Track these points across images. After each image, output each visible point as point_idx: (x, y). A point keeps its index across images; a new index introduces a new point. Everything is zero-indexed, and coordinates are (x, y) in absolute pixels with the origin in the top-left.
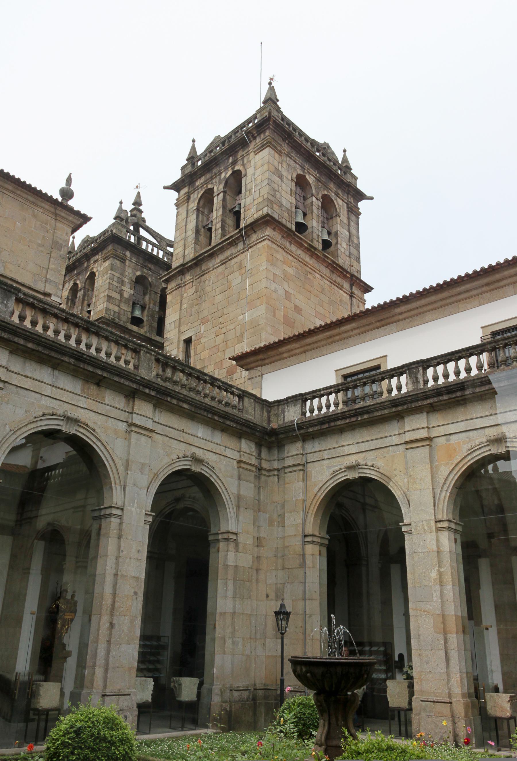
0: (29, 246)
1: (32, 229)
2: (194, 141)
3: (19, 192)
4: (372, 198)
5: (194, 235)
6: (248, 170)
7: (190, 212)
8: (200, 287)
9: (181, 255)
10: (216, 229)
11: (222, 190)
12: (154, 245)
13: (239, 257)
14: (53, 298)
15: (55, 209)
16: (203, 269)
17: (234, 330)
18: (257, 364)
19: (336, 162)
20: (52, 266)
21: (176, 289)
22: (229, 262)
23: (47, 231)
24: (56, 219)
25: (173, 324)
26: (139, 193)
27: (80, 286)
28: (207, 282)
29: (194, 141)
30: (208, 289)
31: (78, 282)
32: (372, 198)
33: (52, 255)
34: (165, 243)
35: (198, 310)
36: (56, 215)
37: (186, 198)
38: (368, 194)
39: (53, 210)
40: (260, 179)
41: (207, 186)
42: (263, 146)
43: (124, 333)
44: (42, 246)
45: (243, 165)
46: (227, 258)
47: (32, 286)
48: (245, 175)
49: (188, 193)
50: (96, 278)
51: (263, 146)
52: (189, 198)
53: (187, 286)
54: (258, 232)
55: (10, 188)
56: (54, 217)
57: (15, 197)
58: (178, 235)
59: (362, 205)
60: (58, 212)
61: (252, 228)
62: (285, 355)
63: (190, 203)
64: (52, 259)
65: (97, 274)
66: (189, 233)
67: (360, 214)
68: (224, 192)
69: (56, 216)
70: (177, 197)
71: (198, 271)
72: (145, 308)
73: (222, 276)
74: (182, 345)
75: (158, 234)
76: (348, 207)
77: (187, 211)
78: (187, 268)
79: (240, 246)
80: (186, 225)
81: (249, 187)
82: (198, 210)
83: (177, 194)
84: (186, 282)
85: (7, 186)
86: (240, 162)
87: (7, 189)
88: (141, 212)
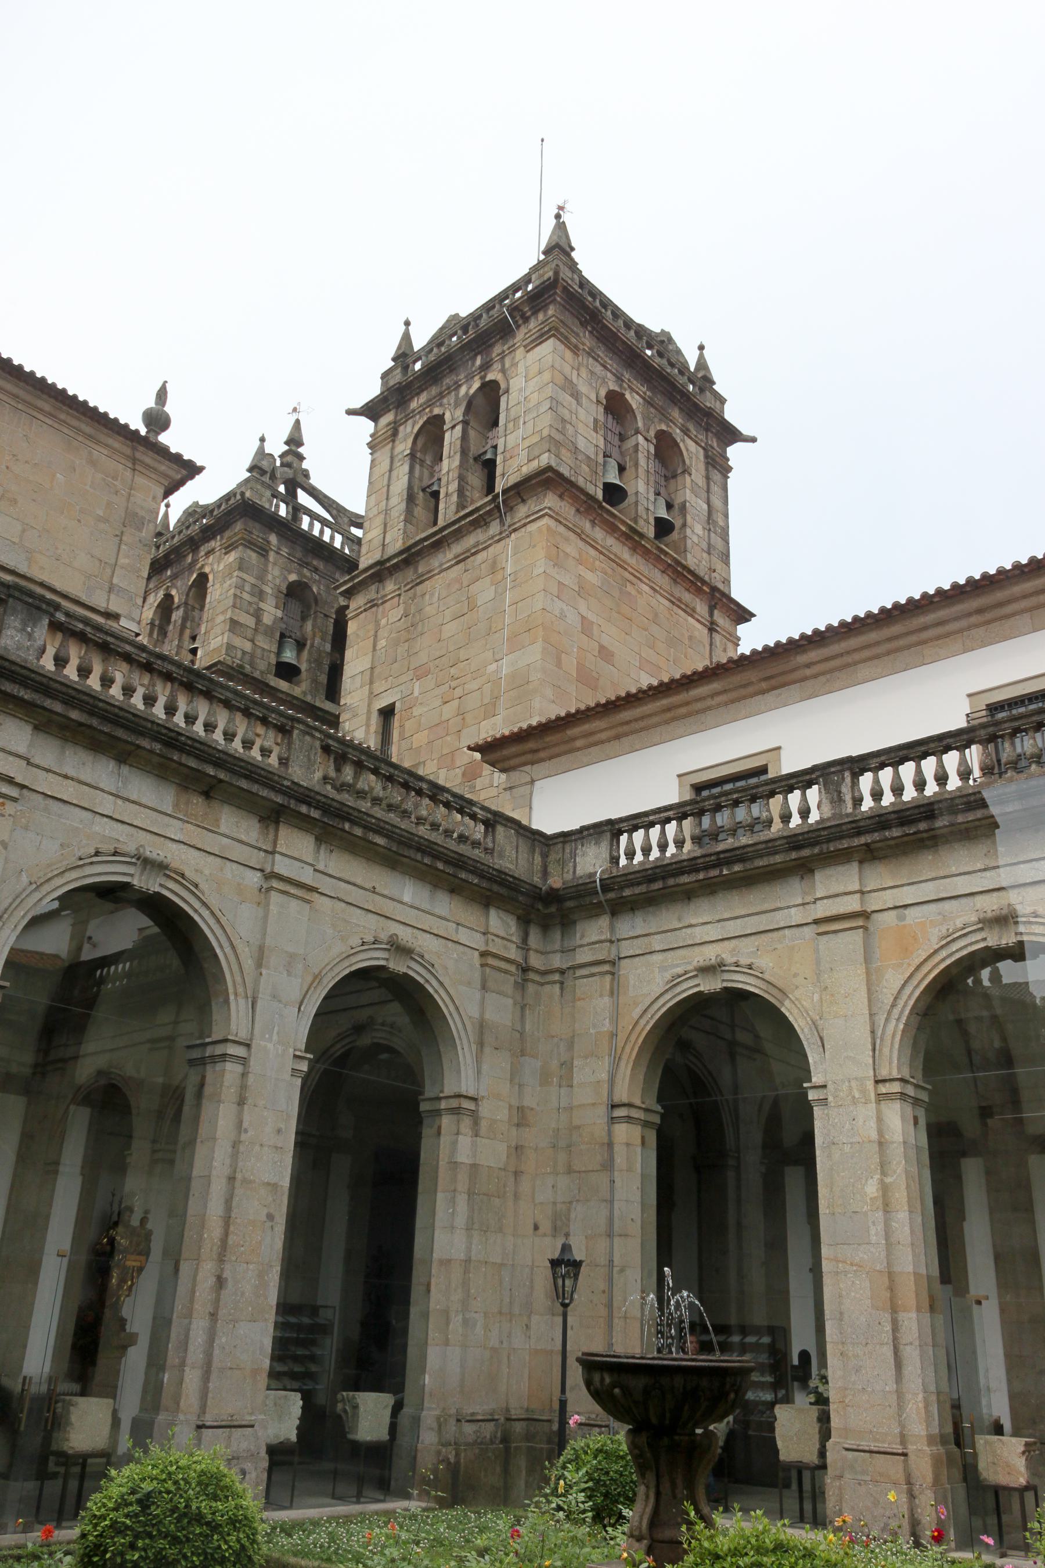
0: (79, 521)
1: (88, 488)
2: (407, 323)
3: (63, 416)
4: (753, 440)
5: (403, 505)
6: (511, 382)
7: (396, 459)
8: (412, 607)
9: (377, 542)
10: (447, 495)
11: (461, 418)
12: (324, 522)
13: (490, 549)
14: (123, 622)
15: (134, 449)
16: (420, 570)
17: (478, 692)
18: (523, 759)
19: (683, 368)
20: (123, 561)
21: (365, 610)
22: (472, 558)
23: (116, 493)
24: (134, 470)
25: (358, 679)
26: (298, 422)
27: (176, 600)
28: (427, 597)
29: (407, 323)
30: (429, 610)
31: (174, 592)
32: (753, 440)
33: (124, 538)
34: (346, 520)
35: (408, 651)
36: (134, 461)
37: (389, 433)
38: (745, 431)
39: (128, 451)
40: (535, 398)
41: (431, 411)
42: (542, 336)
43: (261, 694)
44: (106, 520)
45: (503, 371)
46: (468, 550)
47: (84, 598)
48: (507, 391)
49: (395, 422)
50: (209, 585)
51: (542, 336)
52: (395, 433)
53: (388, 605)
54: (529, 502)
55: (47, 407)
56: (130, 465)
57: (56, 425)
58: (373, 503)
59: (735, 452)
60: (138, 455)
61: (519, 494)
62: (579, 743)
63: (397, 442)
64: (123, 547)
65: (211, 577)
66: (394, 500)
67: (729, 469)
68: (465, 423)
69: (134, 464)
70: (372, 431)
71: (410, 574)
72: (304, 645)
73: (457, 586)
74: (375, 719)
75: (334, 502)
76: (706, 457)
77: (392, 458)
78: (388, 568)
79: (494, 528)
80: (388, 486)
81: (513, 413)
82: (412, 456)
83: (372, 424)
84: (386, 596)
85: (40, 403)
86: (497, 366)
87: (41, 410)
88: (301, 458)
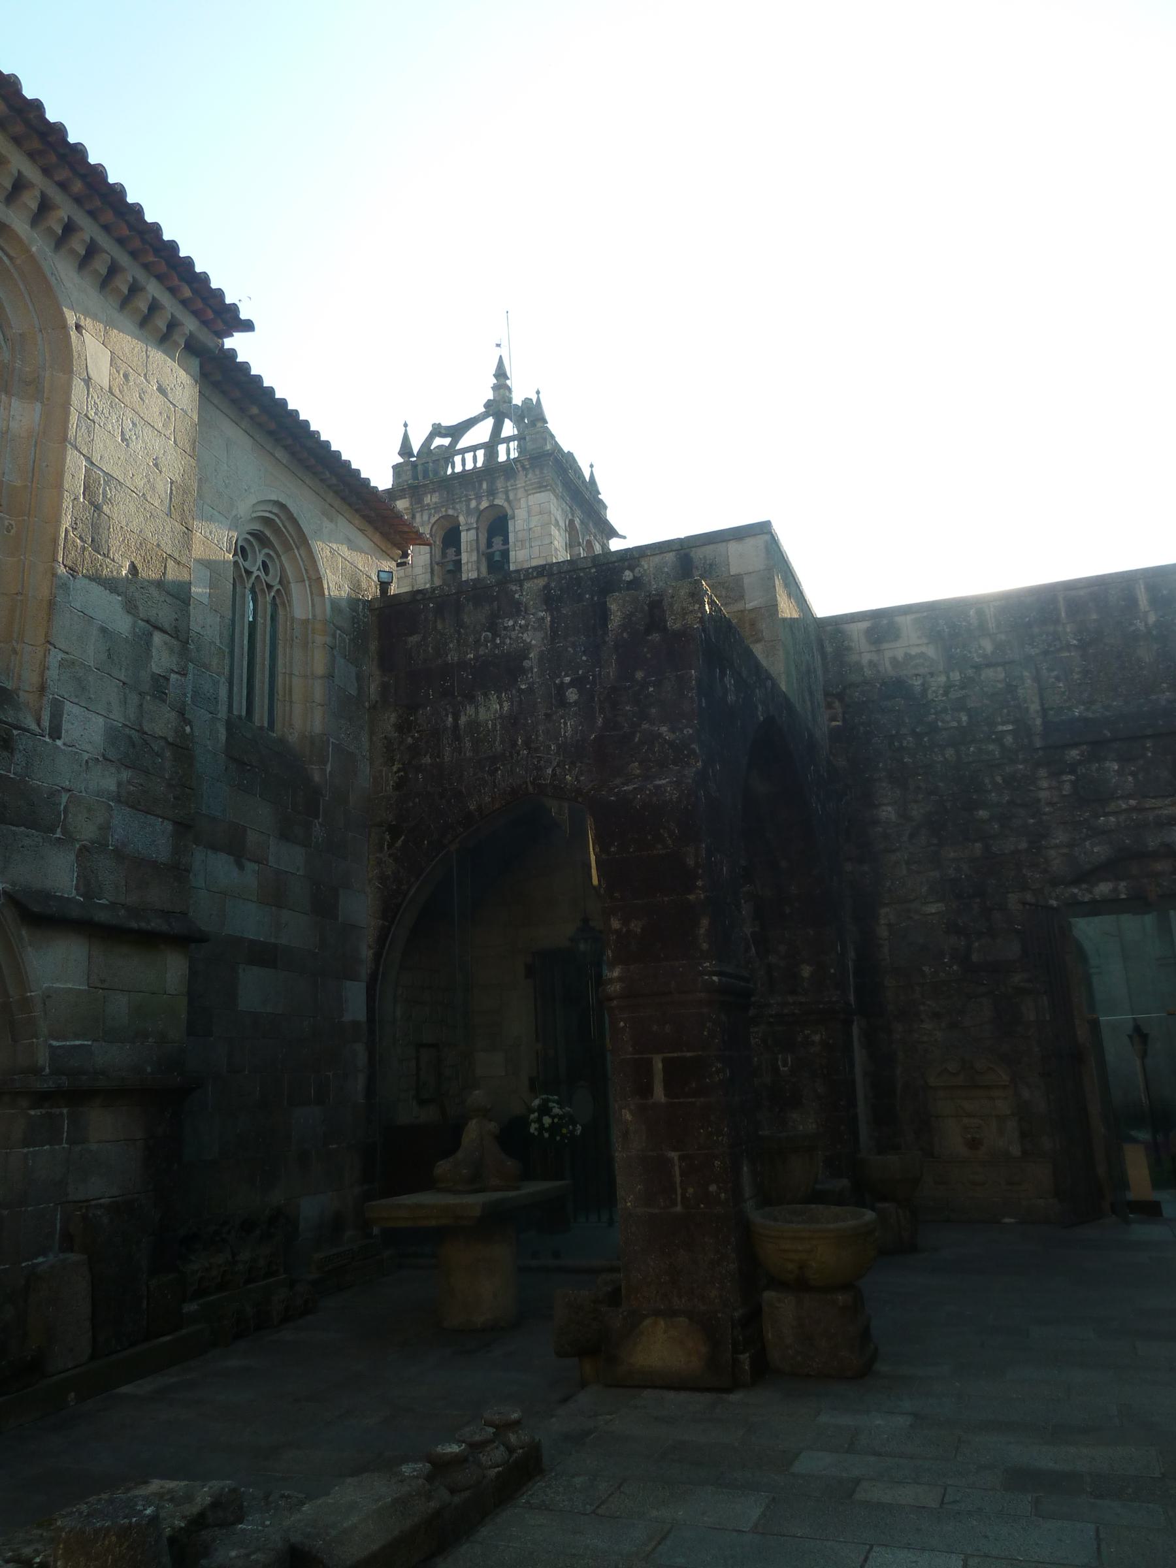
2: (406, 425)
4: (624, 537)
6: (516, 511)
29: (406, 425)
32: (624, 537)
38: (620, 533)
42: (540, 487)
45: (508, 500)
48: (513, 518)
81: (520, 535)
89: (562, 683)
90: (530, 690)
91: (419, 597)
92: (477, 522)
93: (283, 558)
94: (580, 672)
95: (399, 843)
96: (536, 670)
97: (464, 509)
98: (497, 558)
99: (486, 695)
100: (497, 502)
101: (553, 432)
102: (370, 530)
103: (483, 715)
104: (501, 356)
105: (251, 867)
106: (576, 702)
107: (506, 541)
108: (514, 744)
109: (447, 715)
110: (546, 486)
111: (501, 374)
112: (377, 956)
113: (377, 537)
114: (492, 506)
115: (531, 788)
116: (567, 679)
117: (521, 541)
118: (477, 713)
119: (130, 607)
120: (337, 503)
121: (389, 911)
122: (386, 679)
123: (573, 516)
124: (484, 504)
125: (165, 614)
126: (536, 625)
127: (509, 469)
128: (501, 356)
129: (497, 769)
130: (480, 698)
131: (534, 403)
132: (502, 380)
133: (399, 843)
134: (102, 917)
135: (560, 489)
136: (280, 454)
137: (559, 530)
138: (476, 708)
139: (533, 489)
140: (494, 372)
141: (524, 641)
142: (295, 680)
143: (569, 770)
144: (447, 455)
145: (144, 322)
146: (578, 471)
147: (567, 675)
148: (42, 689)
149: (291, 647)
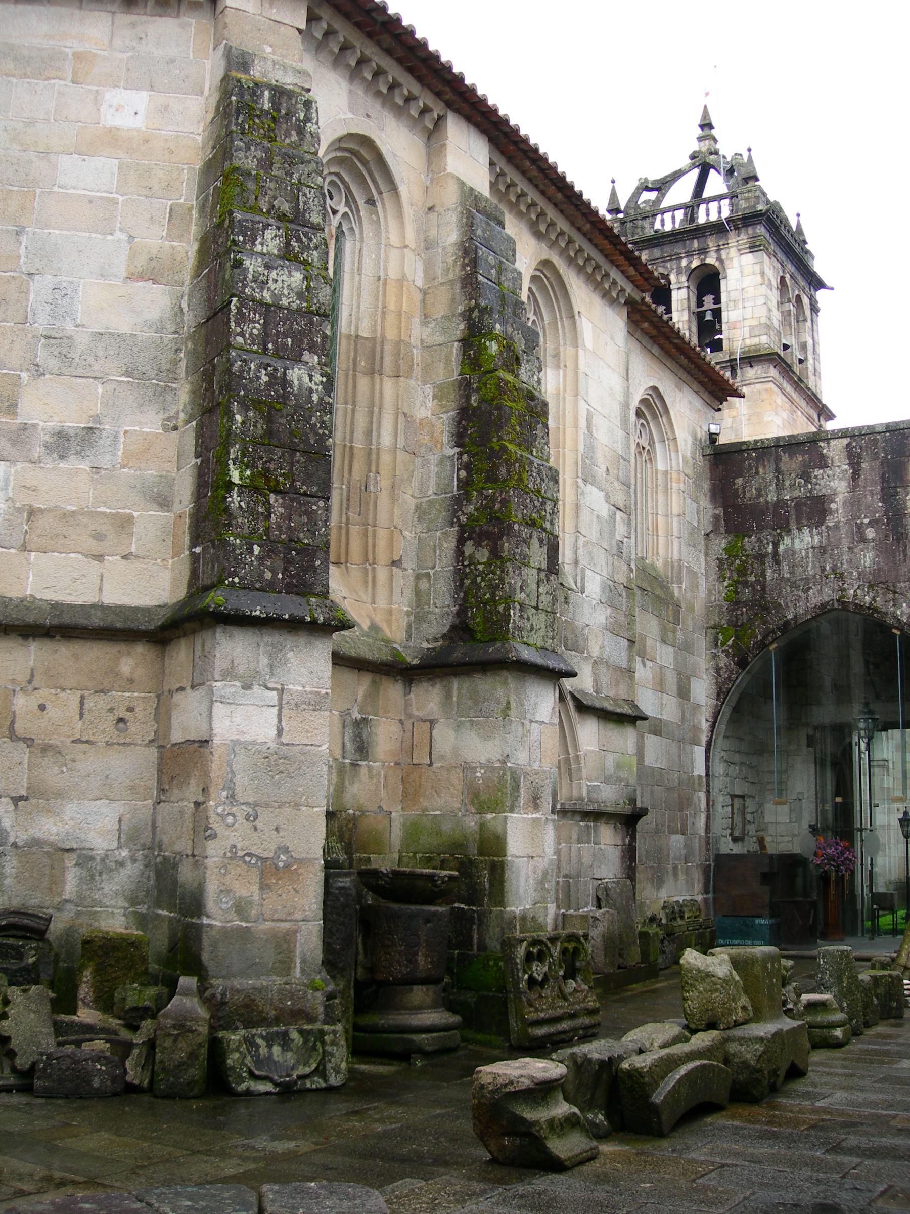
4: (832, 289)
11: (686, 284)
29: (613, 182)
32: (832, 289)
45: (719, 259)
48: (725, 278)
54: (756, 368)
76: (811, 304)
81: (732, 294)
89: (862, 523)
90: (837, 527)
91: (744, 448)
92: (688, 280)
93: (651, 425)
94: (877, 515)
95: (730, 643)
96: (840, 511)
97: (675, 266)
98: (709, 316)
99: (799, 529)
100: (708, 261)
101: (765, 190)
102: (702, 390)
103: (797, 545)
104: (705, 107)
105: (649, 664)
106: (873, 540)
107: (718, 300)
108: (823, 569)
109: (768, 544)
110: (760, 246)
111: (707, 125)
112: (713, 726)
113: (706, 396)
114: (703, 265)
115: (836, 605)
116: (866, 521)
117: (734, 301)
118: (793, 543)
119: (607, 498)
120: (685, 376)
121: (721, 694)
122: (717, 512)
123: (783, 271)
124: (695, 263)
125: (620, 500)
126: (841, 476)
127: (718, 229)
128: (705, 107)
129: (809, 588)
130: (795, 531)
131: (746, 160)
132: (707, 132)
133: (730, 643)
134: (609, 706)
135: (773, 247)
136: (656, 350)
137: (771, 290)
138: (792, 539)
139: (746, 249)
140: (698, 122)
141: (831, 488)
142: (660, 518)
143: (868, 593)
144: (655, 211)
145: (605, 295)
146: (785, 222)
147: (865, 518)
148: (576, 562)
149: (657, 493)
